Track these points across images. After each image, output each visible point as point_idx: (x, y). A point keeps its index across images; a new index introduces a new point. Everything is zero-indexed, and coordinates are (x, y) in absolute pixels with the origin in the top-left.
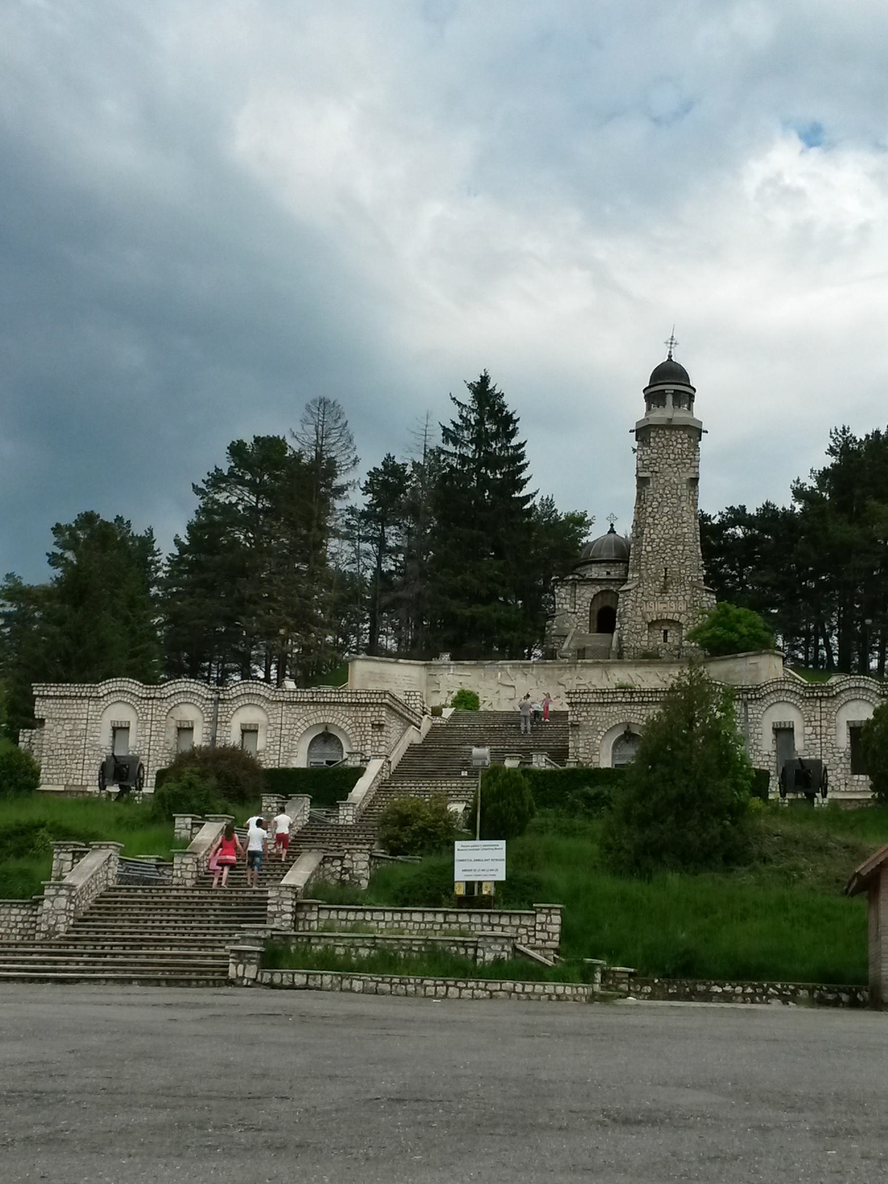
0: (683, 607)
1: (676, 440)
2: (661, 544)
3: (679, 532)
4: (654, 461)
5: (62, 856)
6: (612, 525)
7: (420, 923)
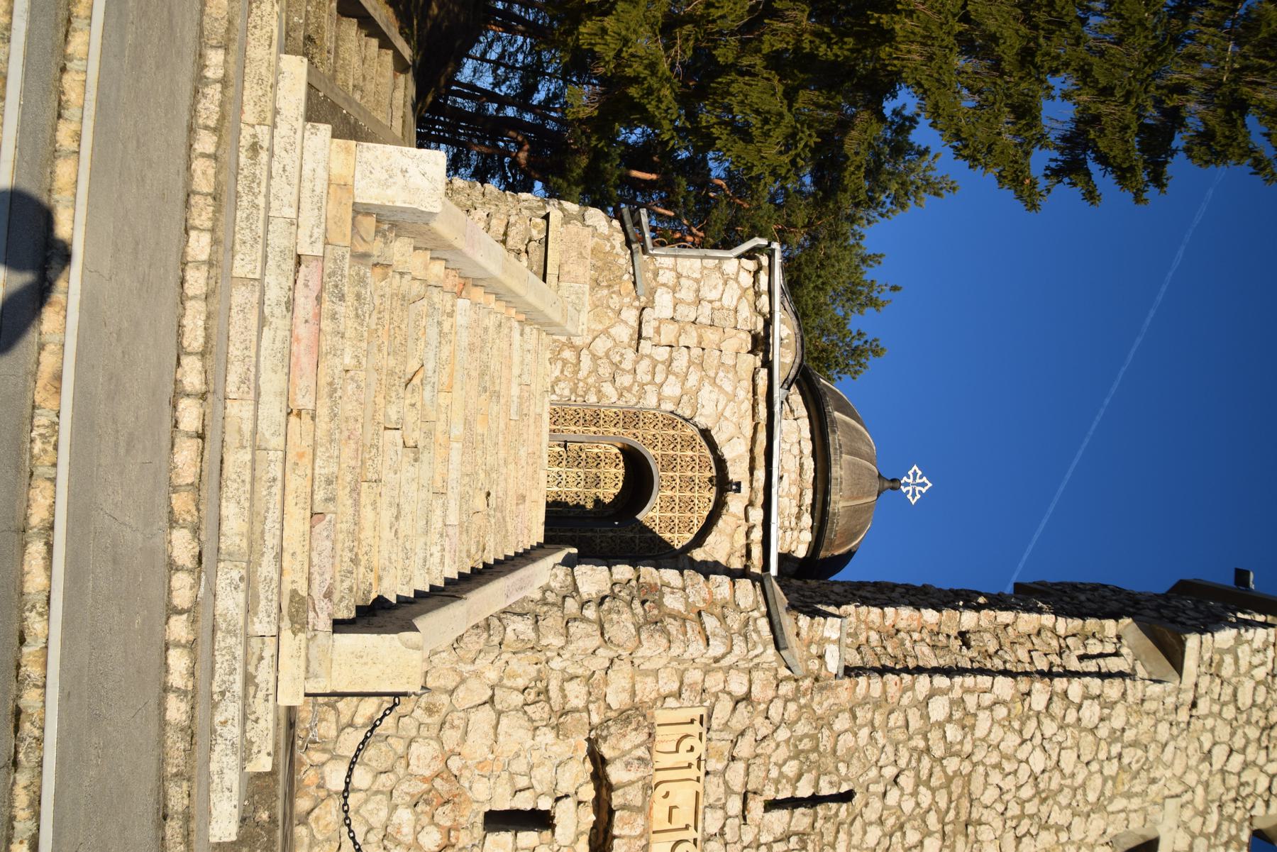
2: (952, 764)
4: (1228, 690)
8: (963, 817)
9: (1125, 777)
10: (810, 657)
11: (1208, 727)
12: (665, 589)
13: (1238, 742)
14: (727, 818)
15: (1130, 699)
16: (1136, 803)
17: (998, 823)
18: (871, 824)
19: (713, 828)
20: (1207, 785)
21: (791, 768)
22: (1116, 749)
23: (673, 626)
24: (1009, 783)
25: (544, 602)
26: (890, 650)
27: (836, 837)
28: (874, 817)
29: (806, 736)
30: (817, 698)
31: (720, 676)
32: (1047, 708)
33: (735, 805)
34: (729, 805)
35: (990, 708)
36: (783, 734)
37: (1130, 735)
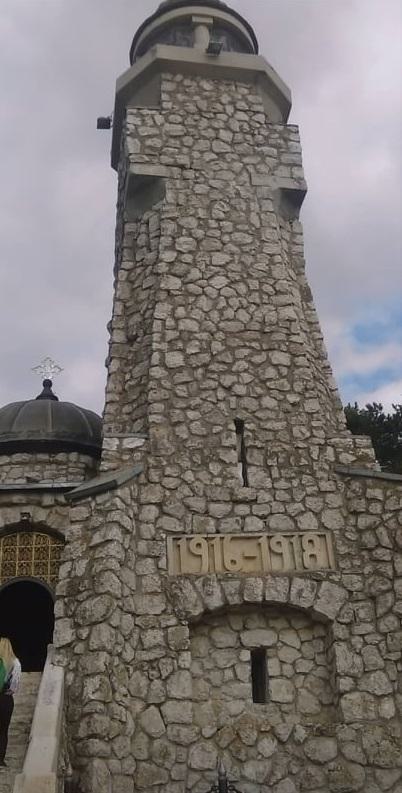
0: (319, 556)
1: (233, 103)
2: (217, 346)
3: (272, 317)
6: (48, 384)
8: (258, 335)
9: (234, 215)
10: (131, 459)
11: (199, 155)
12: (73, 575)
13: (211, 133)
14: (251, 514)
15: (176, 214)
16: (254, 206)
17: (265, 309)
18: (260, 405)
19: (260, 524)
20: (242, 155)
21: (215, 468)
22: (213, 224)
23: (98, 567)
24: (234, 302)
25: (75, 670)
26: (135, 397)
27: (270, 430)
28: (255, 402)
29: (191, 459)
30: (163, 452)
31: (143, 527)
32: (180, 277)
33: (242, 509)
34: (242, 513)
35: (177, 320)
36: (189, 476)
37: (201, 213)
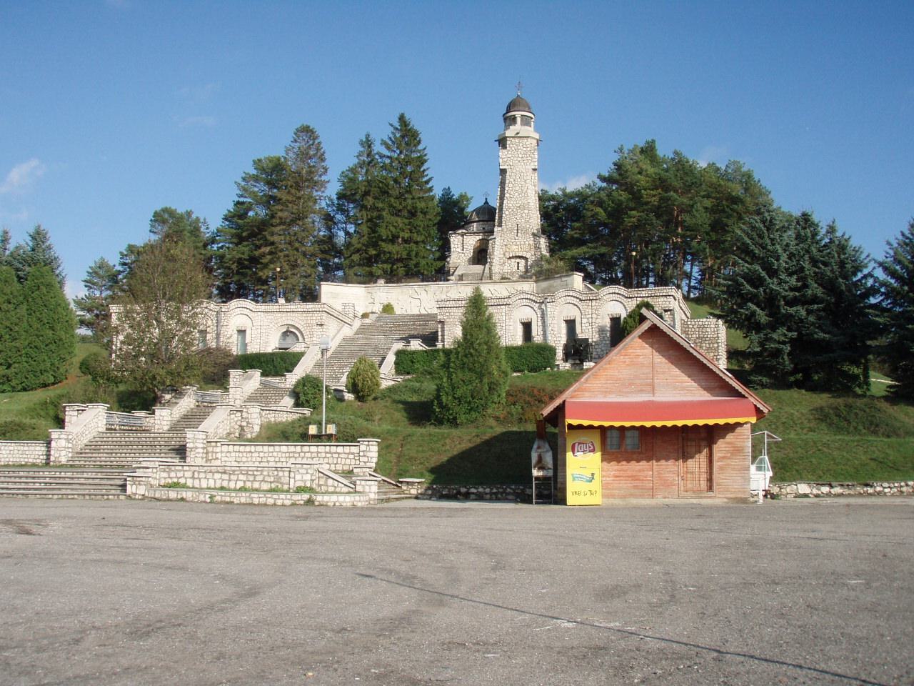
5: (71, 413)
6: (486, 199)
7: (286, 453)
